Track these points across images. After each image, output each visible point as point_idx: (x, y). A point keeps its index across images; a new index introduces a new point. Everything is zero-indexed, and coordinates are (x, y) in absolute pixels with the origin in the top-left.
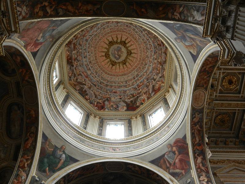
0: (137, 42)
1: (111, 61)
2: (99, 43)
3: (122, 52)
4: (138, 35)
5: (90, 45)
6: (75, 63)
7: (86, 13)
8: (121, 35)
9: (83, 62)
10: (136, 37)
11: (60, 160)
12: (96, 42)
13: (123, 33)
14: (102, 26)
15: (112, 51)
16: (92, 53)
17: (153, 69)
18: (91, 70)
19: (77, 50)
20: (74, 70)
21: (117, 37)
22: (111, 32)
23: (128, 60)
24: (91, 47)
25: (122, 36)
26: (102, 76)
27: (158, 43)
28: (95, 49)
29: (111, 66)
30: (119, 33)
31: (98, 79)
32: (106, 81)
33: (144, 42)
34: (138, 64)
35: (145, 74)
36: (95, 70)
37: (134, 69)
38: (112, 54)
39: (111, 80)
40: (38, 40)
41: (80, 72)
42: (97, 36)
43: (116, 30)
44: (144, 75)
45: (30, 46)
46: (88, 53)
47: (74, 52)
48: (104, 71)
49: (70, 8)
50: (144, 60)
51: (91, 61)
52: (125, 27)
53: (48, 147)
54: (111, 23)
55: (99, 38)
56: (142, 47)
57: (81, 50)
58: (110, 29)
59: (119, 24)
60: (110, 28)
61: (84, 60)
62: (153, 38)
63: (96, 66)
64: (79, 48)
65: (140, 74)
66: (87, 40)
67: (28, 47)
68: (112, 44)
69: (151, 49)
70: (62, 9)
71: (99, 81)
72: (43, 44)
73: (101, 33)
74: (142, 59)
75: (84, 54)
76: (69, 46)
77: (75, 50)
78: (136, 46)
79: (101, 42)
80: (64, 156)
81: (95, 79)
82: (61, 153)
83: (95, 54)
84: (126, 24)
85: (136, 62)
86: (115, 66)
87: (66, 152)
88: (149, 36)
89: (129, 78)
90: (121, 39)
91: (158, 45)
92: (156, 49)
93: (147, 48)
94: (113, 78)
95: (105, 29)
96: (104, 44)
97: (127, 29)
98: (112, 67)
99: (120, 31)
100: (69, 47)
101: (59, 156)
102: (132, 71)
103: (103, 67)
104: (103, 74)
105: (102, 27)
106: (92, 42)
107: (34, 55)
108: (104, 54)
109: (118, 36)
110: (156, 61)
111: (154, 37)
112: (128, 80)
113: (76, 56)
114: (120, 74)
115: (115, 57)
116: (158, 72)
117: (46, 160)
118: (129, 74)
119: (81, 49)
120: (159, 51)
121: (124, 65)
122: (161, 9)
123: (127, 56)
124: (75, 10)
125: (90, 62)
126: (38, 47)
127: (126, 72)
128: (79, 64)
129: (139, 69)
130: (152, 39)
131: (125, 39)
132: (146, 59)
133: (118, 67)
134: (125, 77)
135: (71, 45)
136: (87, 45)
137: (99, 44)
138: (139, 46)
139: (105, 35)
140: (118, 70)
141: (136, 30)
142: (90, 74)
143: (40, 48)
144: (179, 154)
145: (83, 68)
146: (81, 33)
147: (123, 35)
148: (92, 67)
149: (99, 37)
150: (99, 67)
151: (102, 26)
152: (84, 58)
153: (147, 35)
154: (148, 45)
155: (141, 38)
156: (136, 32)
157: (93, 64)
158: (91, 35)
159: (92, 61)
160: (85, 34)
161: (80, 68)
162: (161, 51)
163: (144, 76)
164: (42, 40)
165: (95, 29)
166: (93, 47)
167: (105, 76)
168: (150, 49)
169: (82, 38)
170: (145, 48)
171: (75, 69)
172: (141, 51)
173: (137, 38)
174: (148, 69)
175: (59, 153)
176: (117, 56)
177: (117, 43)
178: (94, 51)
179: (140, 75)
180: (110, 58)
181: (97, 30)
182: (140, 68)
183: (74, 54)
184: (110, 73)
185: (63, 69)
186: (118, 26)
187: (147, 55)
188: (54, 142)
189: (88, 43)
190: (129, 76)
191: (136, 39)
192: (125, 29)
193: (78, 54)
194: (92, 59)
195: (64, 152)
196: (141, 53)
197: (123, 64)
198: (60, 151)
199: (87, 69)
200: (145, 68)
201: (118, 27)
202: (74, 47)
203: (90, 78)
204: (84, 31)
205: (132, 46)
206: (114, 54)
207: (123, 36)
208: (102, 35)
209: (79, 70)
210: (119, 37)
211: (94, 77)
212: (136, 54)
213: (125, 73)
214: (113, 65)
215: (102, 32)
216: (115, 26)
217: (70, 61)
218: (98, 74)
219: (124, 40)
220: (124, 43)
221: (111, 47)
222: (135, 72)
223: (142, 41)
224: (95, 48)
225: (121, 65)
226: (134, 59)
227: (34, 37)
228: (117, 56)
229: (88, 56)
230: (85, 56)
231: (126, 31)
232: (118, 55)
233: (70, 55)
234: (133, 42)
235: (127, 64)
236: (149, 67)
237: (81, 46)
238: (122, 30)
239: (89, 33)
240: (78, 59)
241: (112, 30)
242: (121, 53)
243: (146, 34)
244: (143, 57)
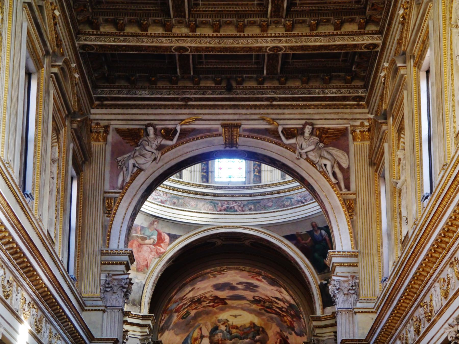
11: (325, 239)
45: (160, 250)
53: (304, 241)
72: (160, 231)
80: (323, 232)
82: (319, 232)
87: (320, 225)
101: (321, 238)
117: (316, 255)
143: (166, 233)
164: (155, 237)
175: (317, 234)
188: (303, 230)
195: (321, 229)
198: (316, 231)
227: (149, 250)
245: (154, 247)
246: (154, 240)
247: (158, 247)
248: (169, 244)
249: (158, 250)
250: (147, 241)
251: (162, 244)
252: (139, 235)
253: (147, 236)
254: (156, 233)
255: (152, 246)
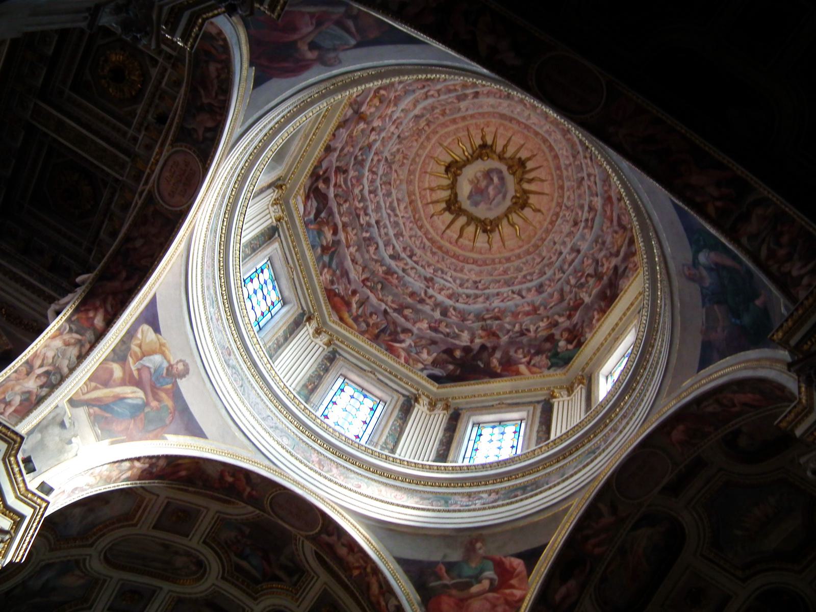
0: (410, 194)
1: (521, 180)
2: (517, 251)
3: (475, 183)
4: (396, 215)
5: (544, 266)
6: (607, 267)
7: (356, 550)
8: (445, 236)
9: (591, 248)
10: (406, 208)
12: (524, 260)
13: (438, 238)
14: (477, 296)
15: (498, 204)
16: (555, 243)
17: (397, 100)
18: (587, 203)
19: (576, 294)
20: (622, 254)
21: (460, 236)
22: (466, 260)
23: (470, 151)
24: (544, 259)
25: (444, 231)
26: (571, 159)
27: (341, 179)
28: (540, 243)
29: (530, 165)
30: (447, 245)
31: (587, 164)
32: (569, 136)
33: (390, 184)
34: (444, 125)
35: (431, 93)
36: (579, 192)
37: (464, 118)
38: (504, 197)
39: (553, 128)
40: (492, 580)
41: (616, 232)
42: (507, 277)
43: (450, 260)
44: (439, 91)
45: (513, 595)
46: (561, 253)
47: (587, 300)
48: (558, 168)
49: (375, 588)
50: (419, 132)
51: (571, 223)
52: (418, 252)
54: (448, 289)
55: (506, 266)
56: (407, 171)
57: (571, 277)
58: (462, 270)
59: (429, 272)
60: (459, 275)
61: (584, 247)
62: (351, 199)
63: (569, 198)
64: (571, 292)
65: (450, 97)
66: (540, 289)
67: (517, 598)
68: (486, 224)
69: (376, 159)
70: (387, 605)
71: (588, 155)
72: (497, 556)
73: (490, 278)
74: (423, 137)
75: (573, 261)
76: (580, 331)
77: (581, 299)
78: (421, 180)
79: (512, 250)
81: (591, 170)
83: (548, 231)
84: (409, 260)
85: (446, 133)
86: (518, 156)
88: (362, 205)
89: (491, 100)
90: (452, 222)
91: (345, 172)
92: (360, 158)
93: (390, 164)
94: (544, 129)
95: (475, 282)
96: (506, 238)
97: (418, 243)
98: (529, 159)
99: (440, 248)
100: (582, 327)
102: (472, 116)
103: (553, 179)
104: (567, 162)
105: (477, 292)
106: (532, 271)
107: (531, 557)
108: (527, 212)
109: (456, 236)
110: (376, 123)
111: (345, 201)
112: (500, 97)
113: (592, 281)
114: (516, 127)
115: (502, 179)
116: (382, 92)
118: (487, 113)
119: (568, 282)
120: (354, 152)
121: (489, 142)
122: (183, 473)
123: (464, 166)
124: (371, 575)
125: (576, 223)
126: (511, 564)
127: (493, 120)
128: (603, 254)
129: (447, 111)
130: (357, 191)
131: (441, 217)
132: (407, 134)
133: (509, 148)
134: (506, 111)
135: (577, 323)
136: (549, 273)
137: (520, 247)
138: (412, 177)
139: (485, 263)
140: (517, 140)
141: (391, 233)
142: (597, 195)
144: (295, 42)
145: (602, 231)
146: (532, 328)
147: (440, 232)
148: (582, 207)
149: (505, 272)
150: (562, 187)
151: (477, 296)
152: (578, 251)
153: (365, 209)
154: (380, 172)
155: (391, 203)
156: (396, 224)
157: (572, 211)
158: (520, 294)
159: (568, 221)
160: (527, 314)
161: (609, 239)
162: (346, 151)
163: (439, 87)
164: (490, 573)
165: (496, 303)
166: (540, 255)
167: (565, 153)
168: (379, 161)
169: (545, 308)
170: (394, 167)
171: (618, 252)
172: (414, 160)
173: (402, 206)
174: (416, 103)
176: (496, 180)
177: (472, 219)
178: (546, 243)
179: (453, 94)
180: (516, 191)
181: (493, 295)
182: (443, 113)
183: (590, 296)
184: (544, 147)
185: (617, 325)
186: (435, 271)
187: (400, 143)
189: (545, 277)
190: (492, 106)
191: (411, 202)
192: (424, 248)
193: (583, 280)
194: (566, 228)
196: (417, 155)
197: (492, 146)
199: (595, 215)
200: (425, 108)
201: (439, 266)
202: (576, 308)
203: (606, 188)
204: (521, 325)
205: (434, 185)
206: (500, 192)
207: (443, 228)
208: (496, 269)
209: (613, 237)
210: (453, 233)
211: (592, 179)
212: (431, 157)
213: (499, 121)
214: (522, 163)
215: (486, 279)
216: (443, 272)
217: (608, 293)
218: (580, 175)
219: (447, 214)
220: (452, 205)
221: (495, 219)
222: (463, 109)
223: (394, 192)
224: (537, 247)
225: (499, 149)
226: (450, 144)
228: (496, 180)
229: (569, 246)
230: (574, 255)
231: (425, 240)
232: (492, 180)
233: (596, 306)
234: (422, 197)
235: (478, 142)
236: (411, 106)
237: (562, 290)
238: (434, 250)
239: (517, 306)
240: (594, 264)
241: (461, 264)
242: (478, 181)
243: (370, 211)
244: (416, 140)
245: (496, 595)
246: (492, 580)
247: (508, 591)
248: (529, 575)
249: (509, 598)
250: (475, 589)
251: (514, 582)
252: (447, 581)
253: (471, 577)
254: (490, 564)
255: (490, 595)
